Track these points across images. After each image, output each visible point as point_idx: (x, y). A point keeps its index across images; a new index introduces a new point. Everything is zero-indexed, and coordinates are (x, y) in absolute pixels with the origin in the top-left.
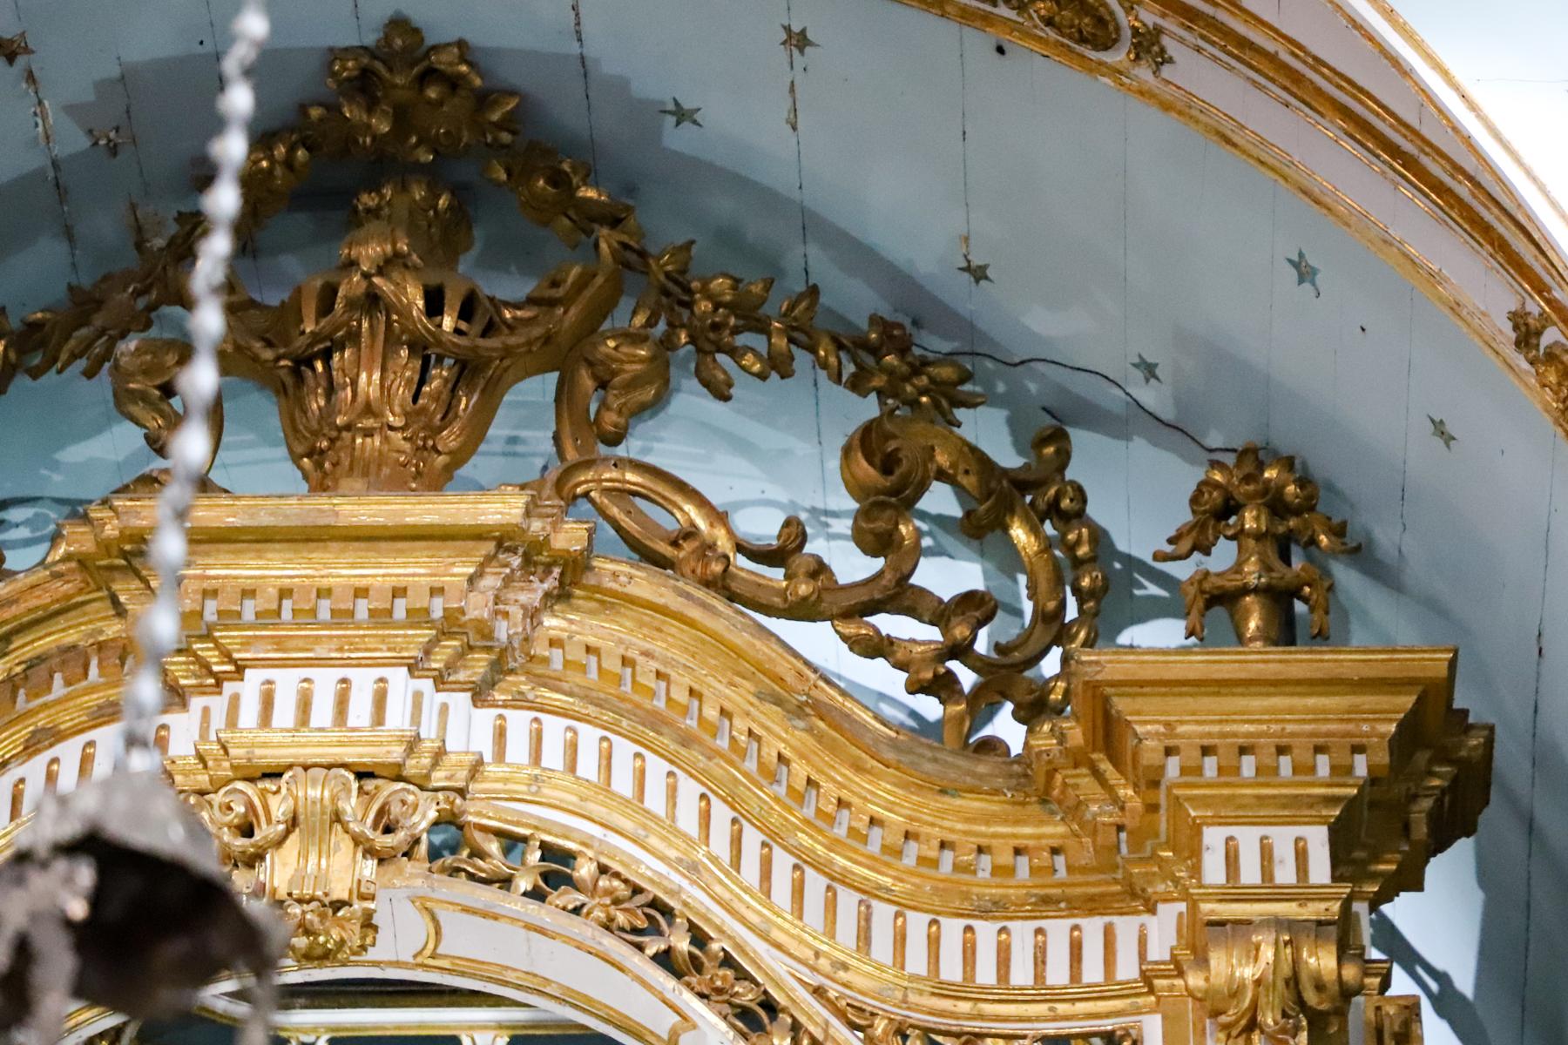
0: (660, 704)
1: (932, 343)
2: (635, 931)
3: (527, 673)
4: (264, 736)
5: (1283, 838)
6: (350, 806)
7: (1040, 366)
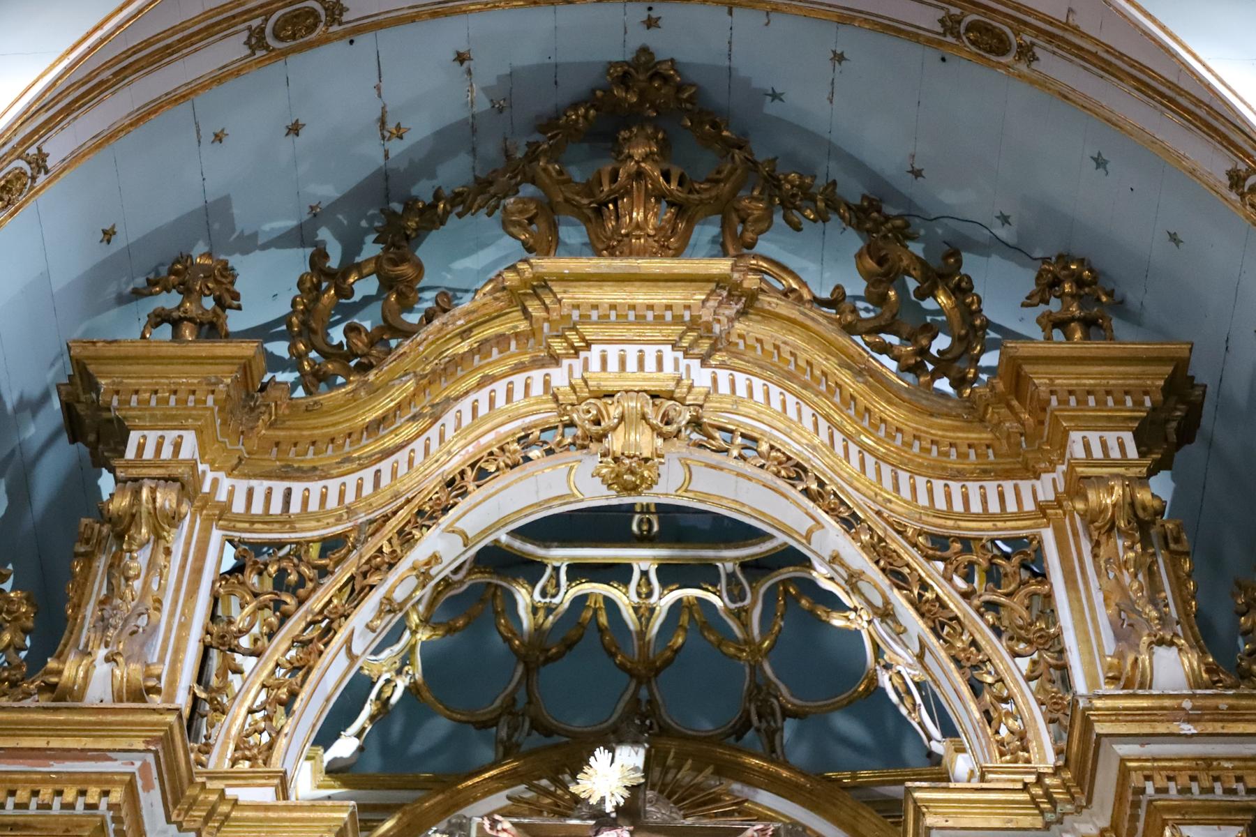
0: (792, 367)
1: (889, 210)
2: (789, 478)
3: (727, 351)
4: (604, 375)
5: (1111, 437)
6: (649, 410)
7: (945, 220)
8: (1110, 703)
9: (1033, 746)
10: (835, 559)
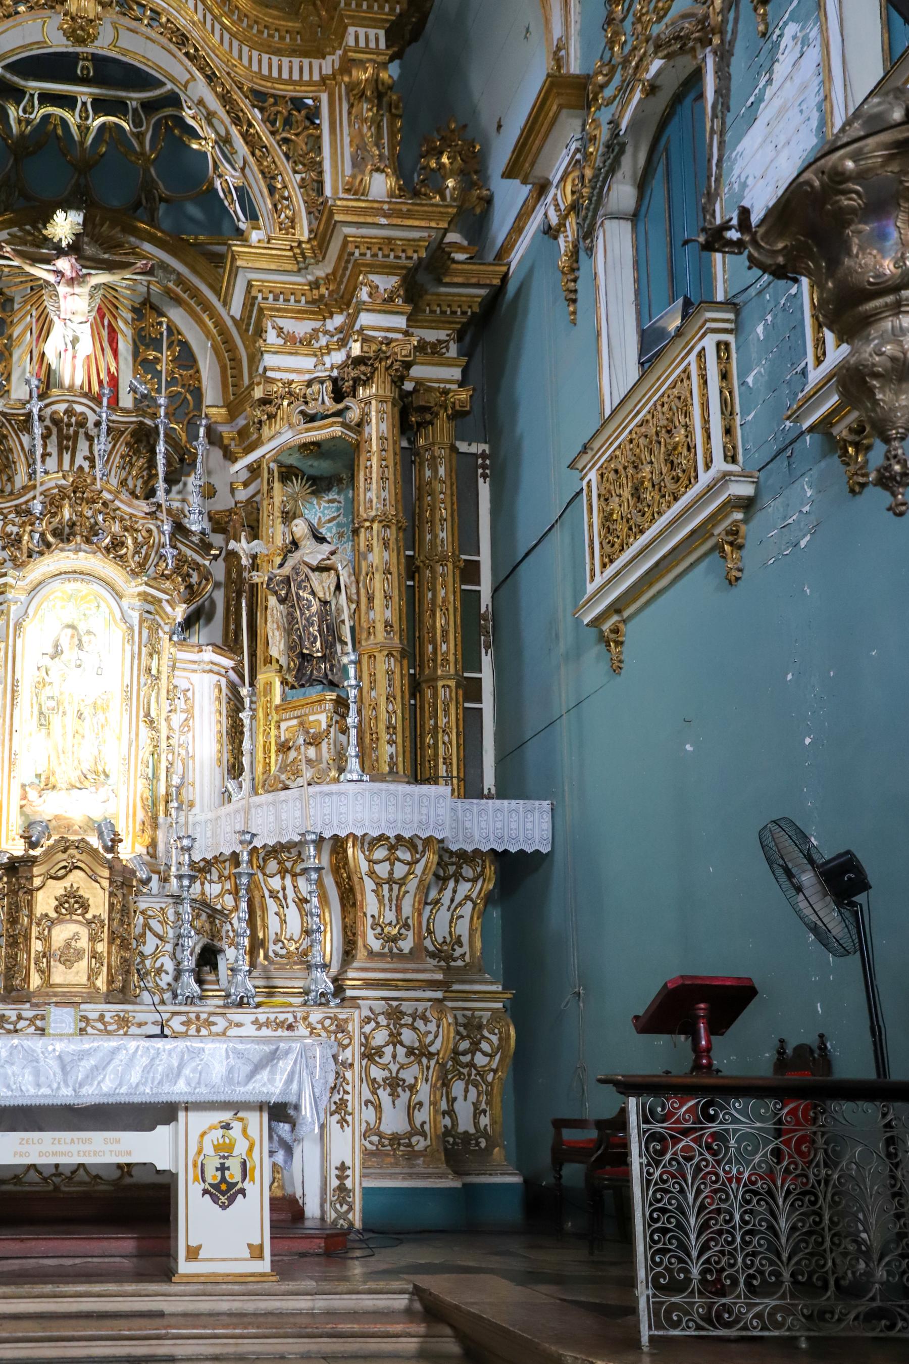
8: (345, 203)
9: (298, 226)
10: (201, 102)
